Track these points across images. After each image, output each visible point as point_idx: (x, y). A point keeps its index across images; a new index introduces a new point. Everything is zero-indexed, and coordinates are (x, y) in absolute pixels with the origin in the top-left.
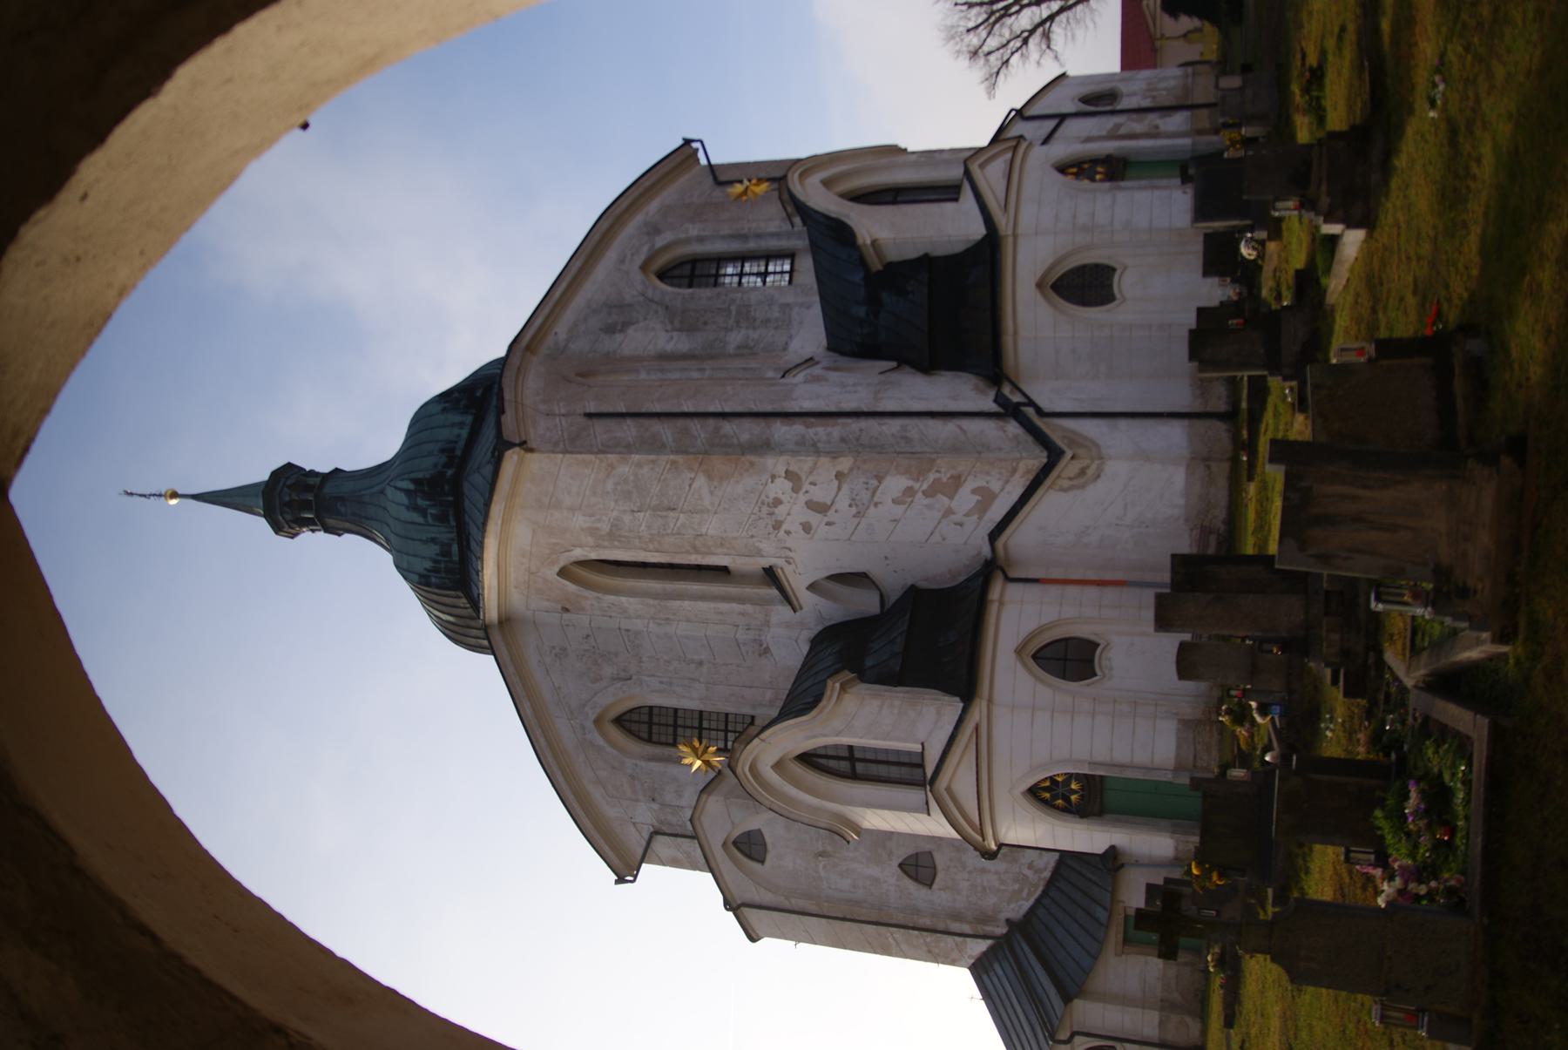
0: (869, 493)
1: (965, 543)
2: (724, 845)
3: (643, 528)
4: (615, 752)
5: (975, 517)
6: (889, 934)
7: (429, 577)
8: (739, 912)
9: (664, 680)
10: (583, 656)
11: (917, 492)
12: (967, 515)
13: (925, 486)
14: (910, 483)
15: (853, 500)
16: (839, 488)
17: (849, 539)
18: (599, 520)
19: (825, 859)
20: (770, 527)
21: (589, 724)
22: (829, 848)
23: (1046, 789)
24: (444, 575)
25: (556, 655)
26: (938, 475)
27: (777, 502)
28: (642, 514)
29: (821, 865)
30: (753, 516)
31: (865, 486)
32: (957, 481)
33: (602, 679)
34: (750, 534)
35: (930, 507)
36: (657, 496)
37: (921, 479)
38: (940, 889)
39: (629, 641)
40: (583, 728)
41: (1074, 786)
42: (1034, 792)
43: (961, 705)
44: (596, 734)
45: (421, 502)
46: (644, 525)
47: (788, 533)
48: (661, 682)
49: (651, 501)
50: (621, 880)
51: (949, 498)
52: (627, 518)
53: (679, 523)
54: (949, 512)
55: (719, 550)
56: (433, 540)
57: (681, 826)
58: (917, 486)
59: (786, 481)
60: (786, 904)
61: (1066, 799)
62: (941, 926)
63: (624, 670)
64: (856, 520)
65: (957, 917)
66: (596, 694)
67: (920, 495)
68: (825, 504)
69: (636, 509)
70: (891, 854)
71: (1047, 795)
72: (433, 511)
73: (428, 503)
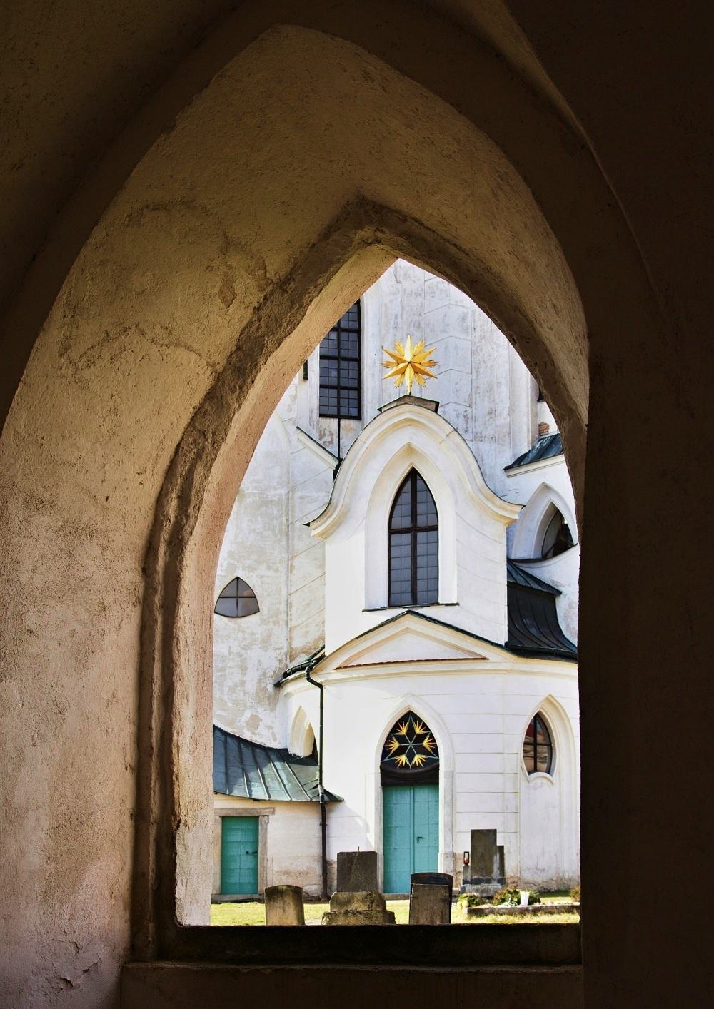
9: (399, 320)
22: (249, 500)
23: (411, 730)
41: (418, 758)
42: (410, 718)
43: (503, 644)
48: (396, 318)
61: (400, 751)
70: (252, 569)
71: (404, 731)
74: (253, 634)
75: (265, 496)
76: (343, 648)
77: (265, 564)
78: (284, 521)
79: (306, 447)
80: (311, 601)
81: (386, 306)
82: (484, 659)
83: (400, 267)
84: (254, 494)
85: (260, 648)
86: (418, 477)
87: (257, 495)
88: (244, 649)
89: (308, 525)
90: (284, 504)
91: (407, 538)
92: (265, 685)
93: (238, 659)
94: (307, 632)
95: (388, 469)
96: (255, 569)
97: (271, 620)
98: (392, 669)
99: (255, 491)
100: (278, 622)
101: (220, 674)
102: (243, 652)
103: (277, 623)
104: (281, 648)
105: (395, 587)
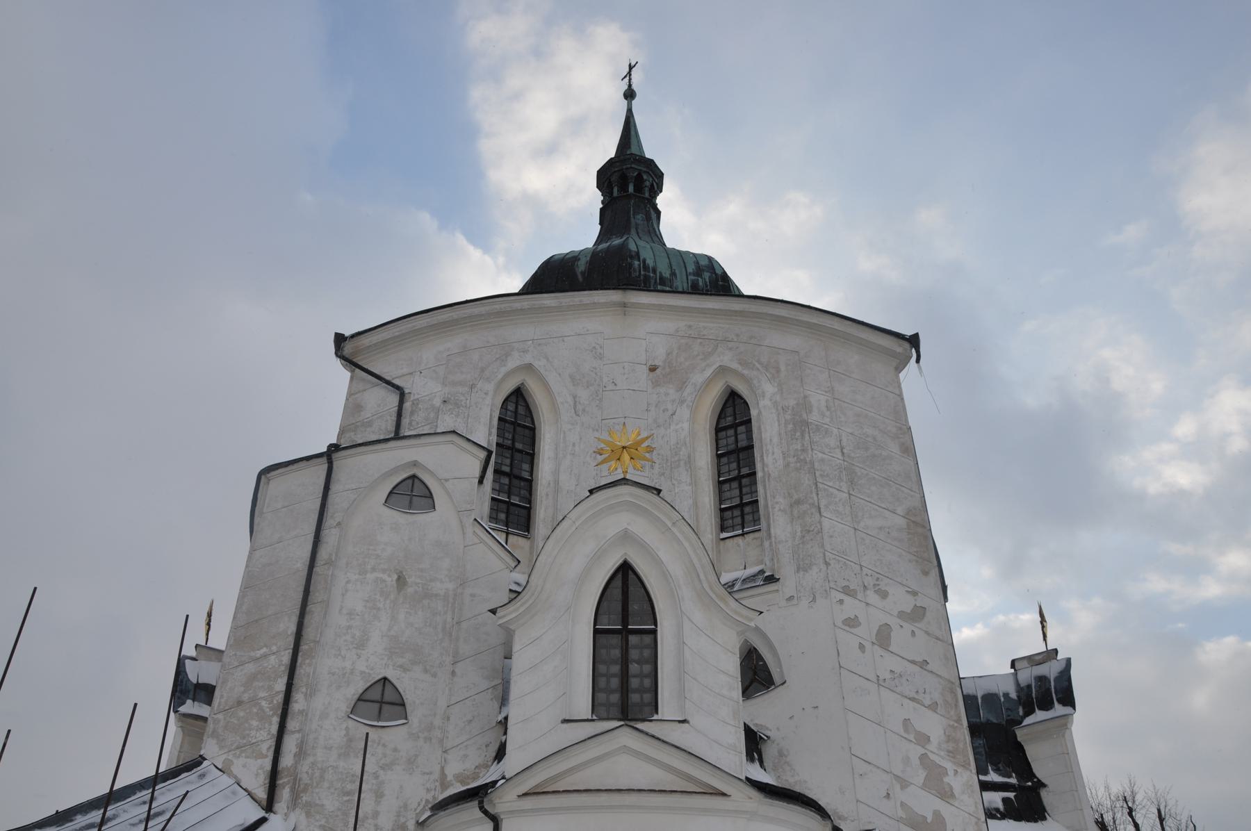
0: (913, 694)
1: (857, 801)
2: (415, 464)
3: (820, 455)
4: (500, 376)
5: (901, 813)
6: (274, 648)
7: (639, 261)
8: (324, 459)
10: (596, 374)
11: (923, 747)
12: (903, 804)
13: (932, 756)
14: (935, 740)
15: (901, 676)
16: (913, 662)
17: (840, 667)
18: (823, 415)
19: (394, 582)
20: (846, 583)
21: (528, 359)
22: (410, 590)
24: (642, 273)
25: (594, 347)
26: (951, 773)
27: (884, 595)
28: (839, 456)
29: (385, 577)
30: (858, 567)
31: (921, 691)
32: (946, 795)
33: (574, 385)
34: (832, 562)
35: (906, 761)
36: (867, 474)
37: (942, 753)
38: (347, 729)
39: (614, 423)
40: (525, 351)
44: (518, 363)
45: (707, 275)
46: (824, 456)
47: (841, 602)
48: (574, 445)
49: (857, 466)
50: (340, 339)
51: (924, 784)
52: (832, 442)
53: (836, 492)
54: (904, 784)
55: (800, 529)
56: (673, 274)
57: (410, 424)
58: (933, 746)
59: (912, 607)
60: (329, 522)
62: (291, 724)
63: (584, 410)
64: (873, 677)
65: (301, 753)
66: (560, 374)
67: (923, 751)
68: (889, 645)
69: (845, 451)
70: (405, 670)
72: (701, 284)
73: (707, 280)
74: (395, 750)
75: (430, 588)
76: (534, 767)
77: (421, 665)
78: (449, 619)
79: (482, 541)
80: (474, 717)
81: (564, 433)
82: (724, 794)
83: (580, 403)
84: (417, 584)
85: (404, 770)
86: (630, 572)
87: (420, 585)
88: (382, 768)
89: (493, 611)
90: (451, 600)
91: (615, 640)
92: (405, 819)
93: (374, 782)
94: (466, 756)
95: (597, 557)
96: (408, 670)
97: (420, 734)
98: (603, 799)
99: (418, 581)
100: (431, 739)
101: (346, 798)
102: (381, 772)
103: (428, 739)
104: (431, 773)
105: (601, 697)
